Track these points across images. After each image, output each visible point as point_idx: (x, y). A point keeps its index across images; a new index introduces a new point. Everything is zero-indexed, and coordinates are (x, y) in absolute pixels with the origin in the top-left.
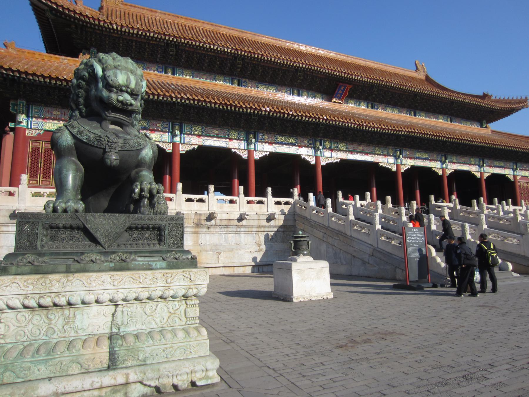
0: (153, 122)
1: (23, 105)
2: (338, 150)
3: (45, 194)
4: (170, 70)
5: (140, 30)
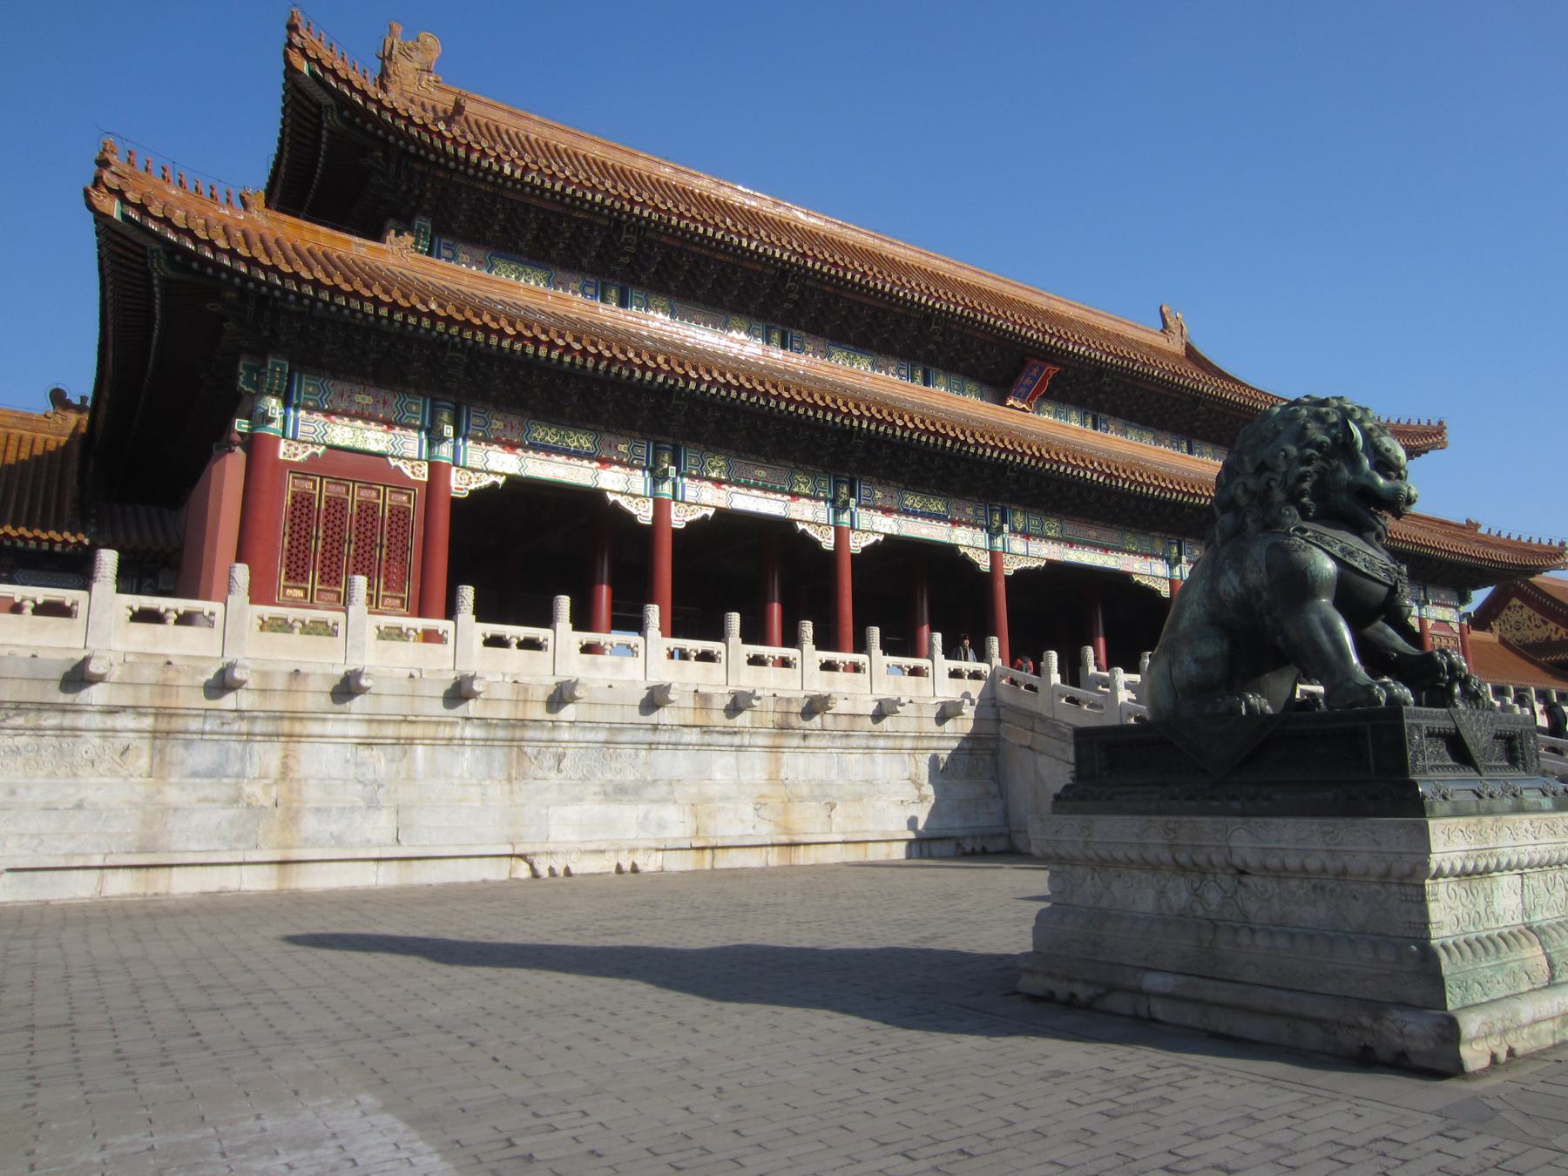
0: (608, 438)
1: (281, 373)
2: (1043, 537)
3: (412, 633)
4: (613, 293)
5: (572, 183)
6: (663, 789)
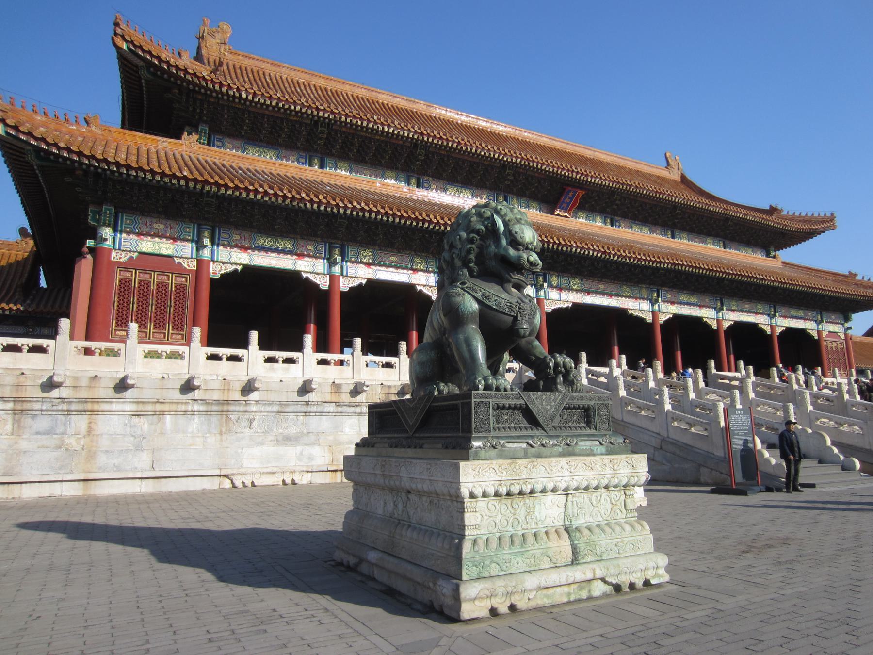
0: (301, 242)
1: (110, 213)
2: (570, 289)
3: (164, 354)
4: (316, 161)
6: (312, 438)
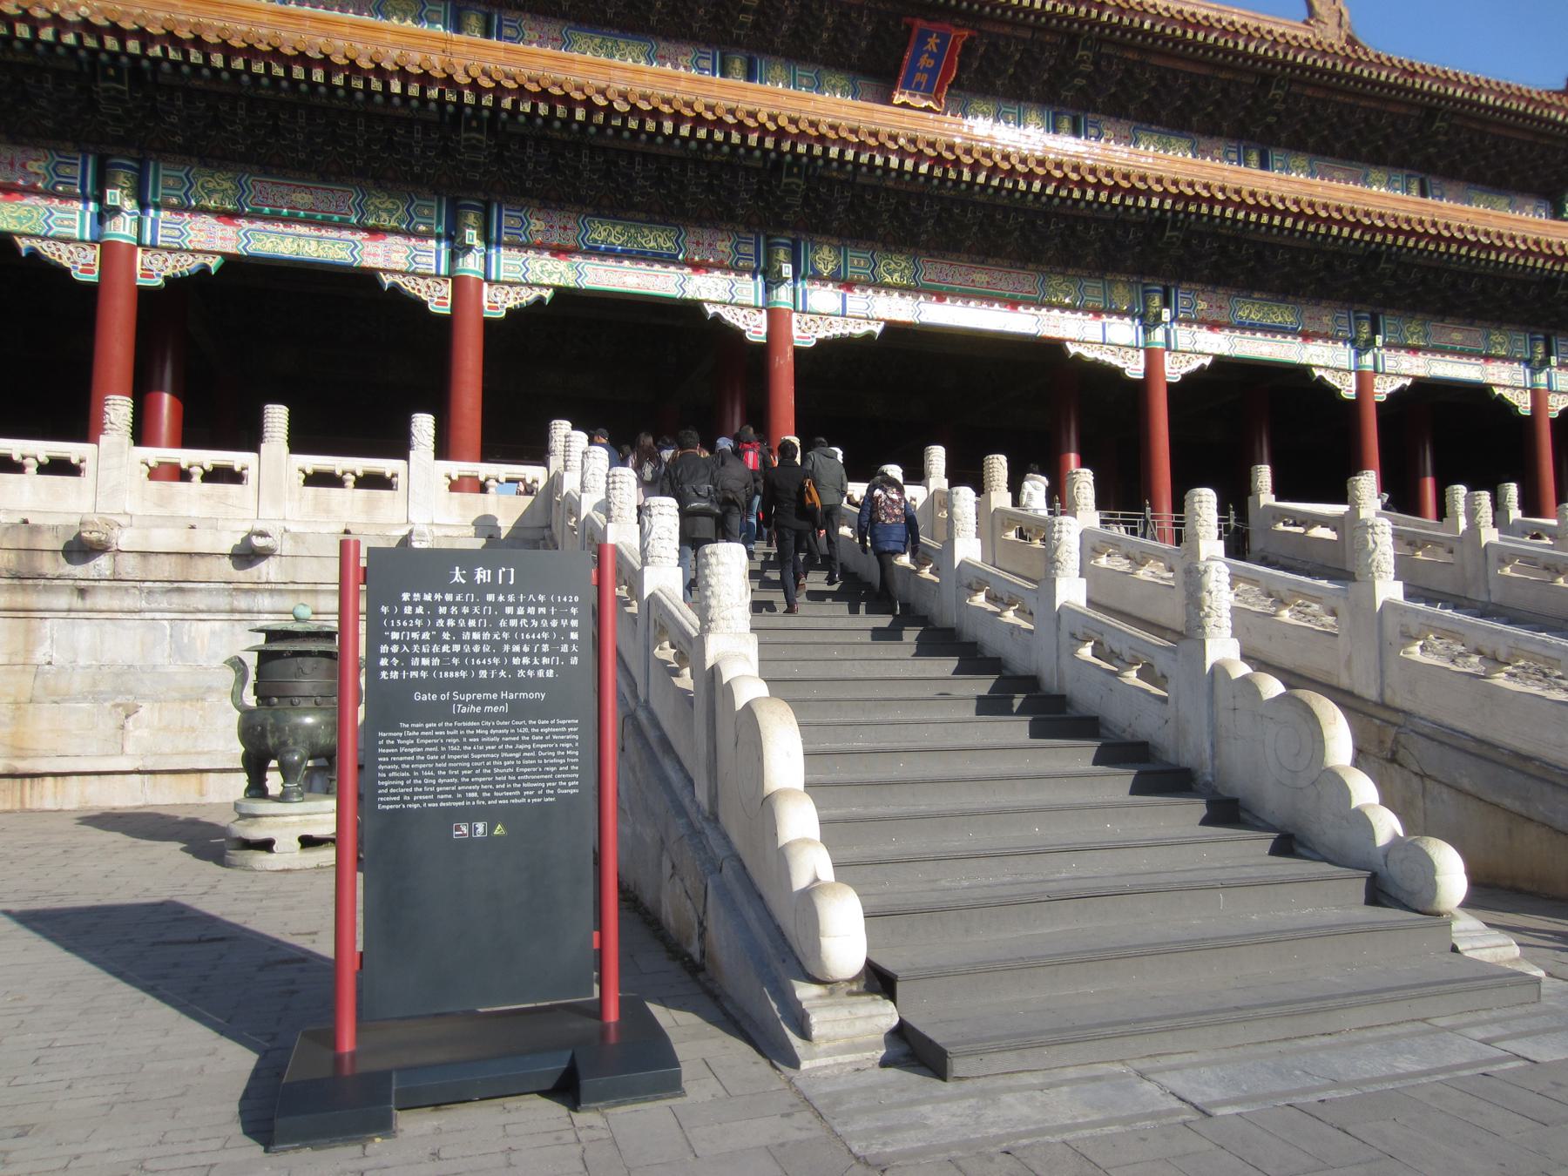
2: (878, 285)
